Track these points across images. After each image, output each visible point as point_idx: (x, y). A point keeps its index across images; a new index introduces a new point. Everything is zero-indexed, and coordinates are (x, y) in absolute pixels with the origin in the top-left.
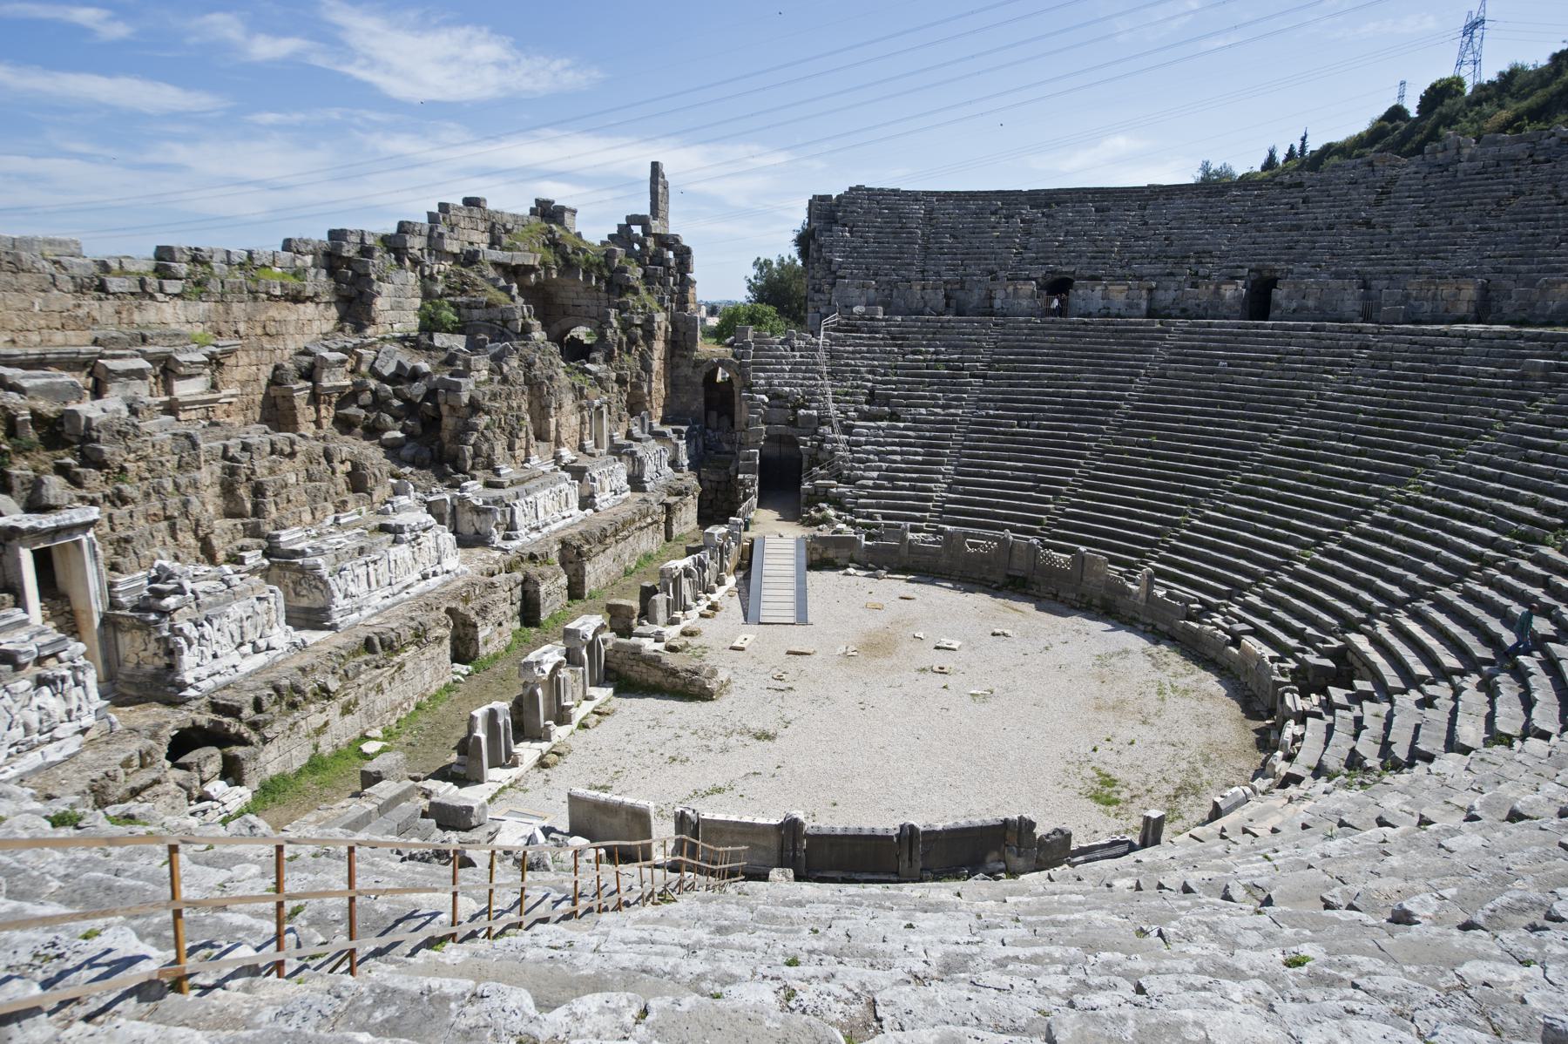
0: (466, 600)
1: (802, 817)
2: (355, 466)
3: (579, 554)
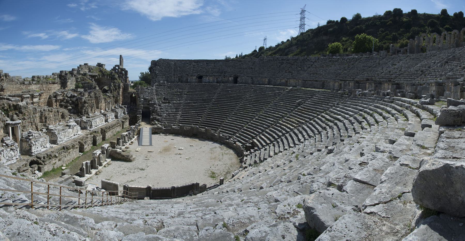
1: (151, 186)
3: (105, 131)
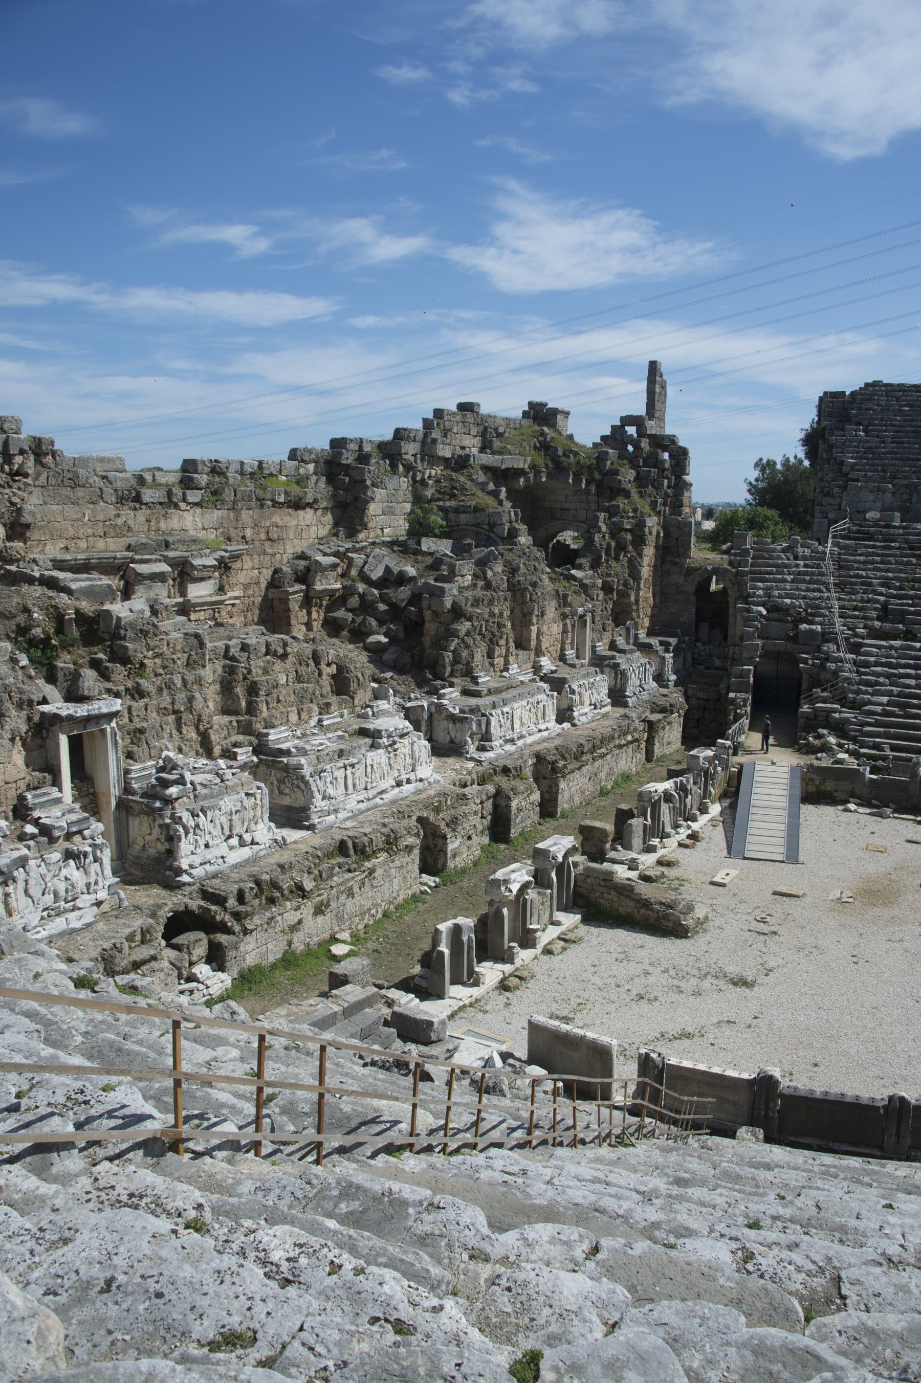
0: (437, 810)
1: (777, 1073)
2: (340, 669)
3: (554, 770)
